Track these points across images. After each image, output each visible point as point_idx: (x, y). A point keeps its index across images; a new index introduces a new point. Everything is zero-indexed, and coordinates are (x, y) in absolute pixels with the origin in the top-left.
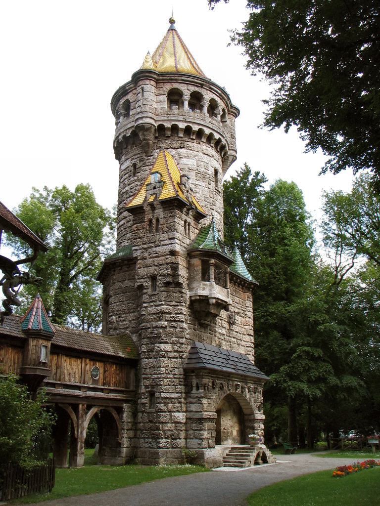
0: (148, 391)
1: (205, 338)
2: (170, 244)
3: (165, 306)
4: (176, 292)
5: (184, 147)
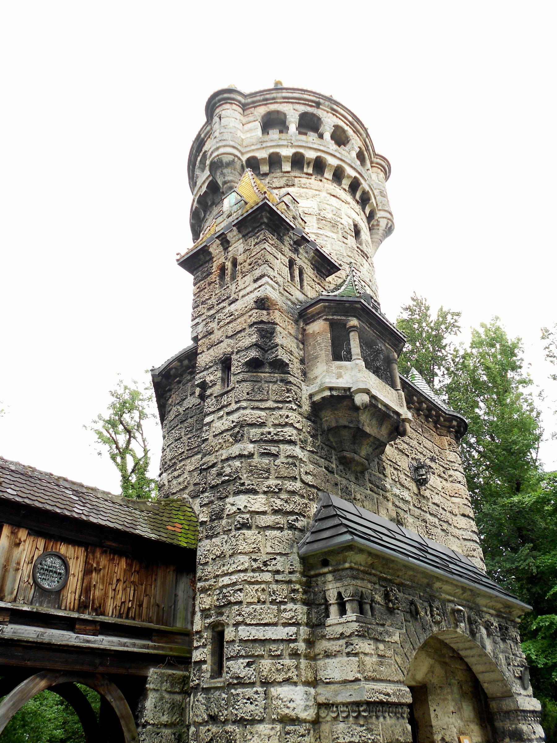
0: (210, 624)
1: (358, 497)
2: (255, 289)
3: (248, 411)
4: (275, 382)
5: (293, 185)
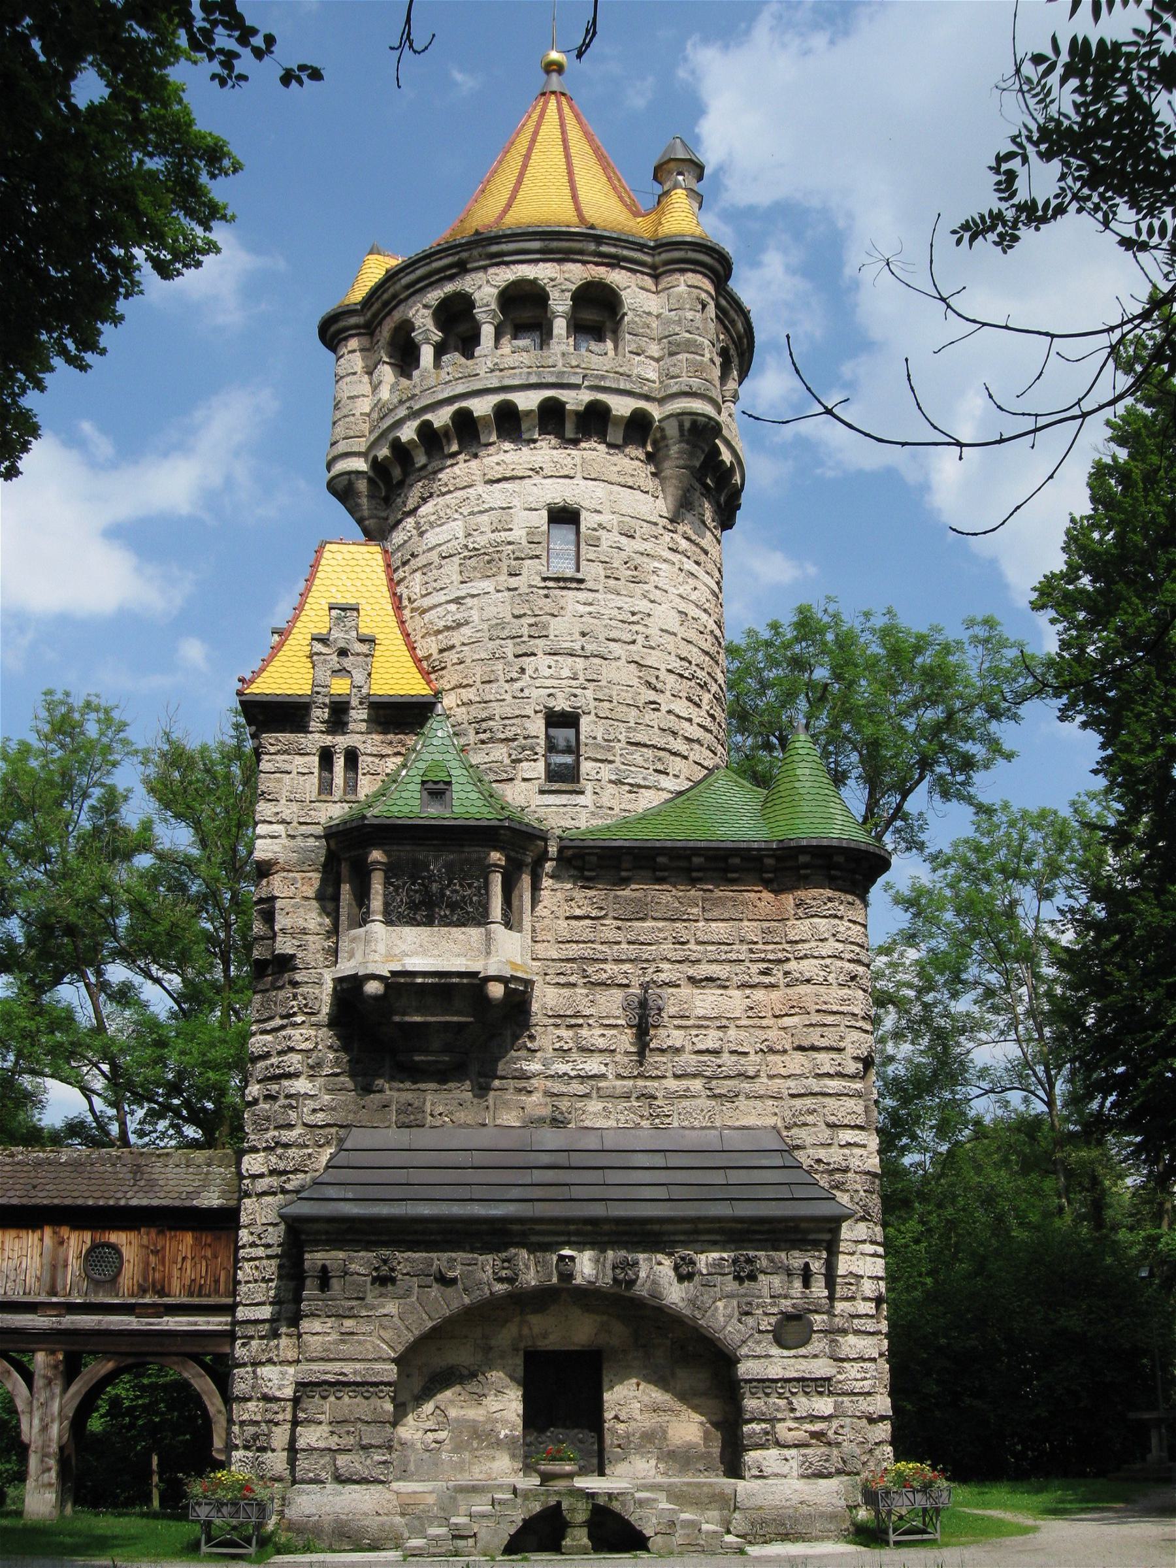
5: (431, 495)
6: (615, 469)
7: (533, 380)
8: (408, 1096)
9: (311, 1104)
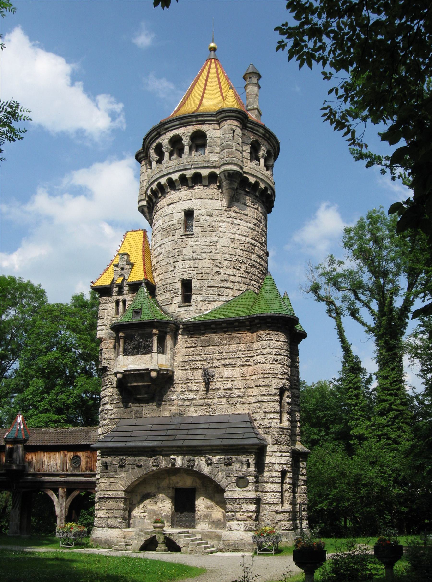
6: (206, 194)
7: (176, 169)
8: (138, 408)
9: (111, 412)
